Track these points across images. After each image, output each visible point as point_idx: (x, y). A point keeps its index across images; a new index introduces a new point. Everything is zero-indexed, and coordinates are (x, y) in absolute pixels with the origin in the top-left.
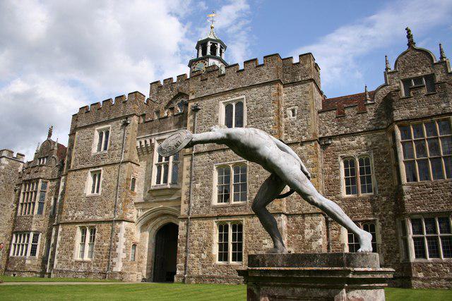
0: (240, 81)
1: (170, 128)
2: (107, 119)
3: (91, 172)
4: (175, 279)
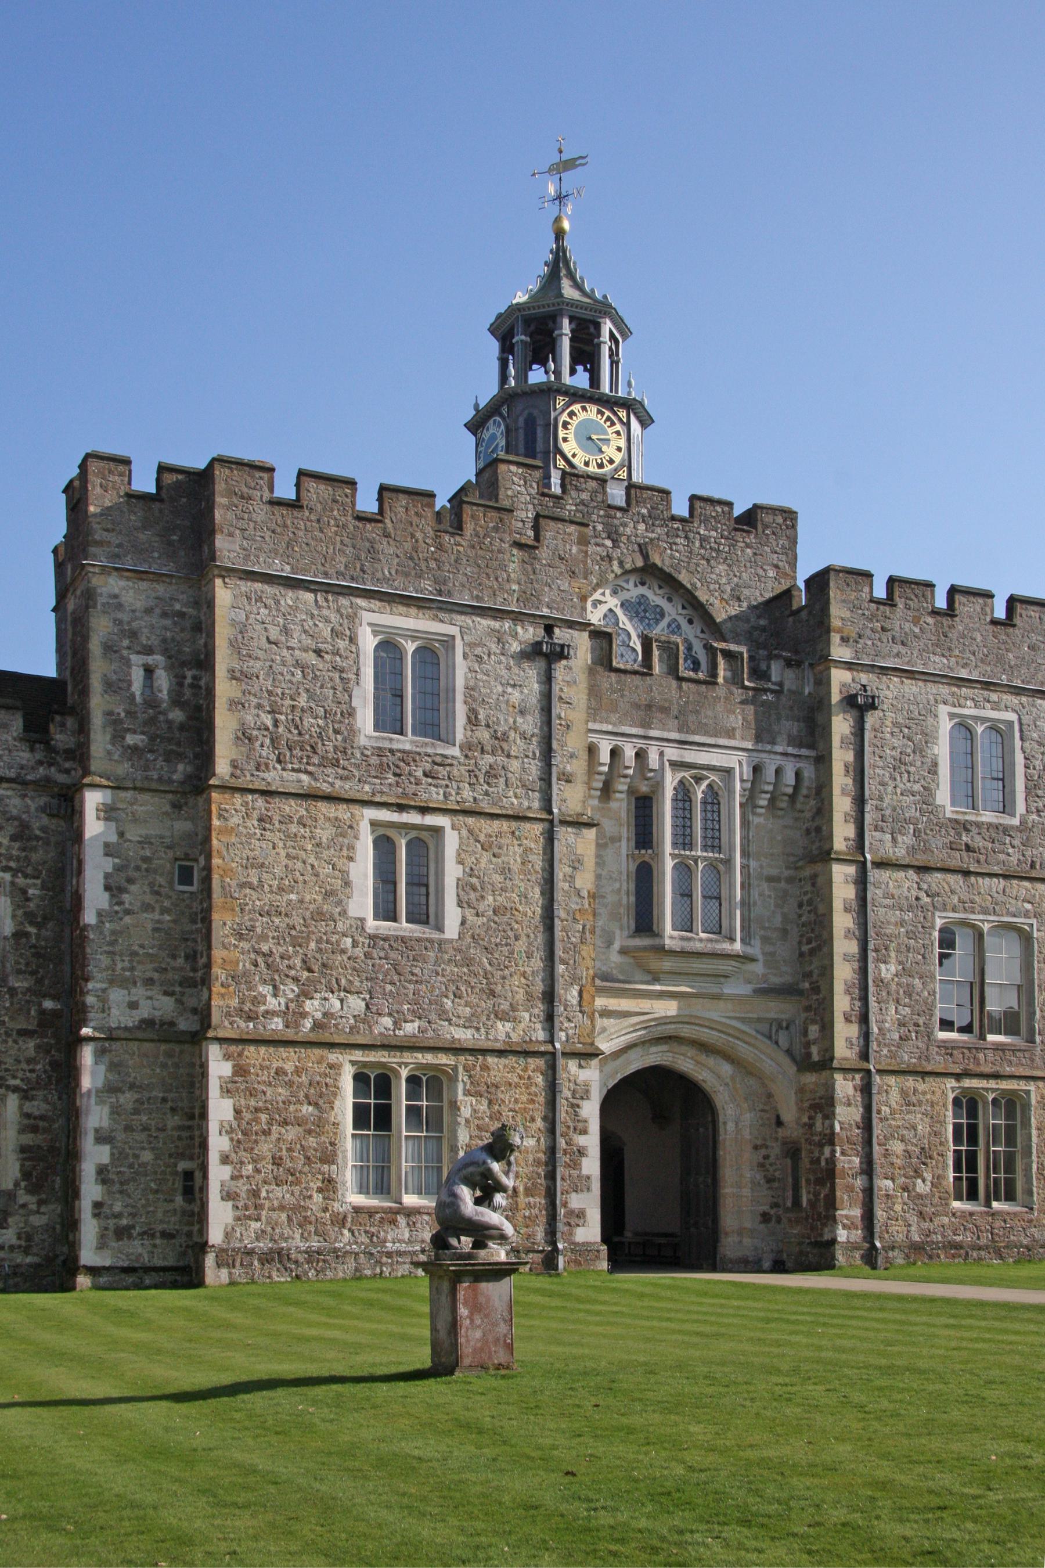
0: (1000, 660)
1: (730, 734)
2: (426, 588)
3: (374, 824)
4: (841, 1258)
